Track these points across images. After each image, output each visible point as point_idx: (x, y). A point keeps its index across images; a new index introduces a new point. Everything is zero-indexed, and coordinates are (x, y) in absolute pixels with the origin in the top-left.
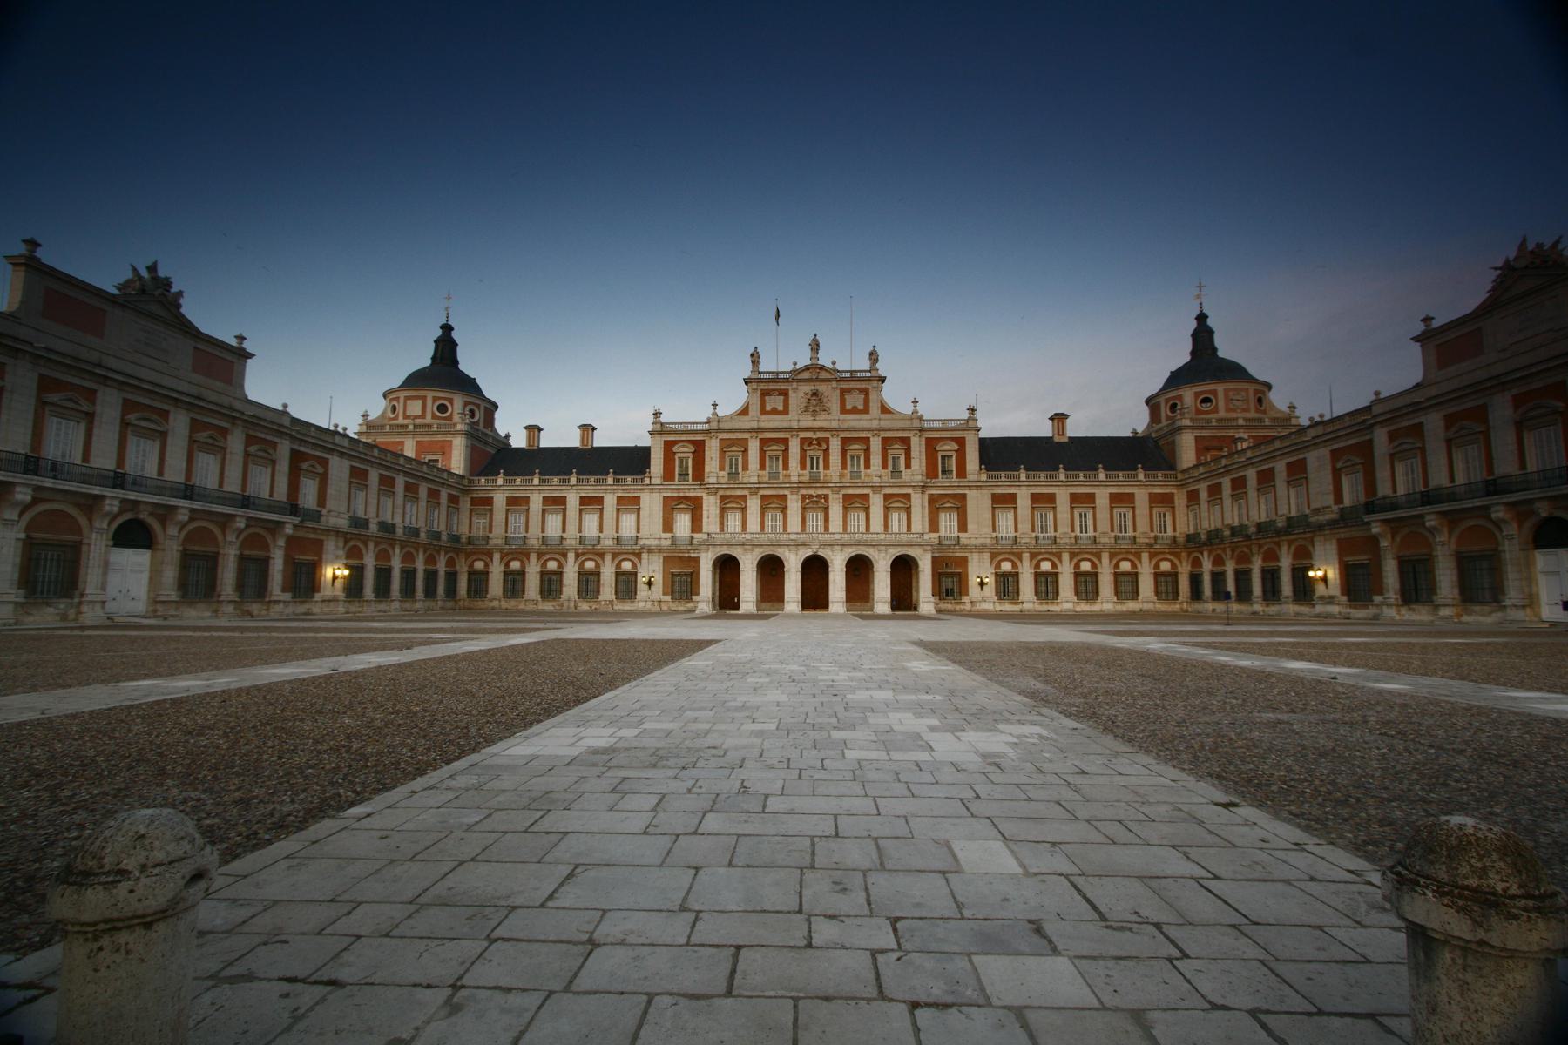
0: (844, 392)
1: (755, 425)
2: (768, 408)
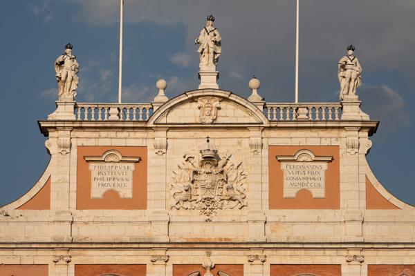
0: (279, 156)
1: (62, 232)
2: (97, 192)
